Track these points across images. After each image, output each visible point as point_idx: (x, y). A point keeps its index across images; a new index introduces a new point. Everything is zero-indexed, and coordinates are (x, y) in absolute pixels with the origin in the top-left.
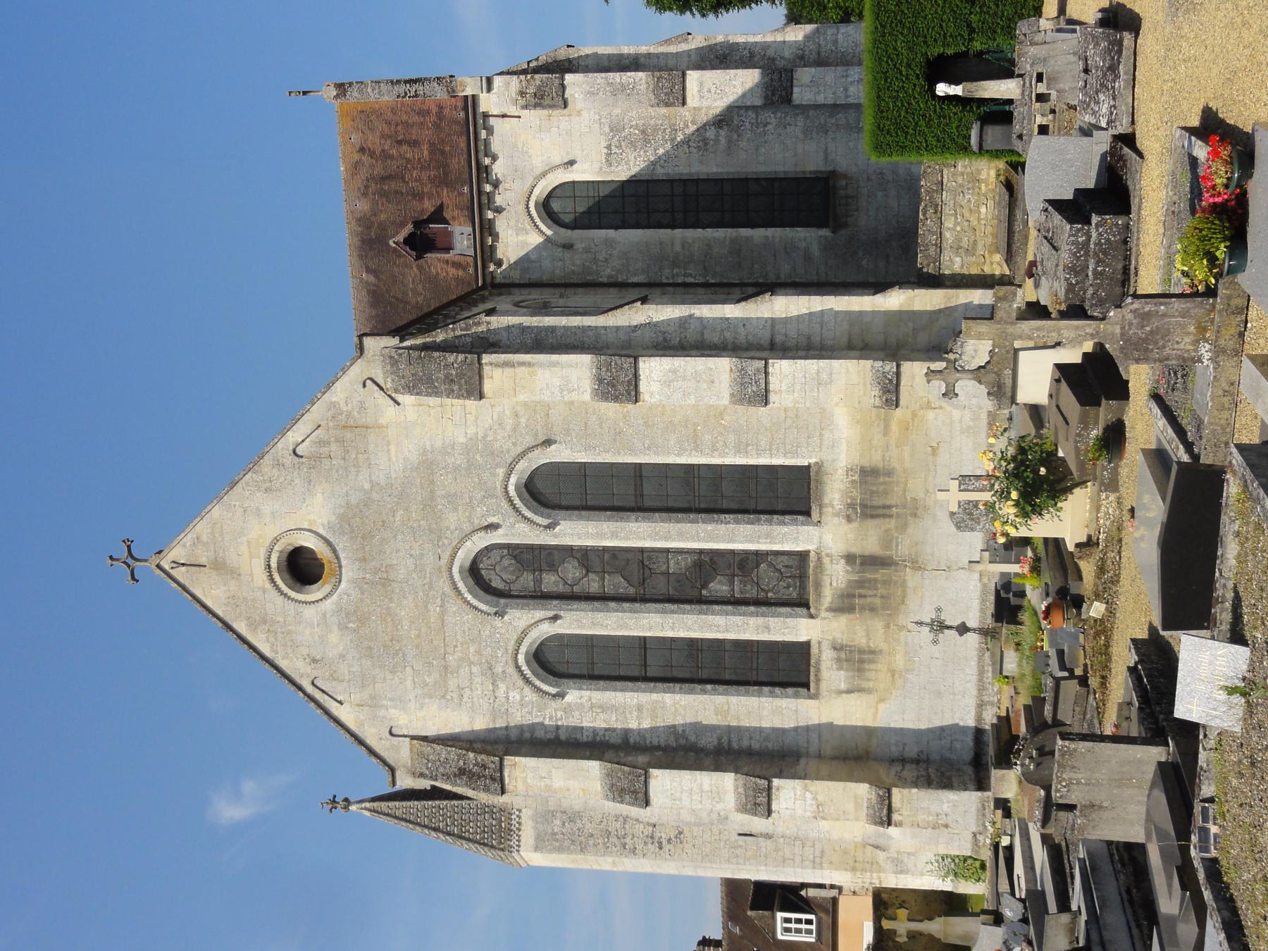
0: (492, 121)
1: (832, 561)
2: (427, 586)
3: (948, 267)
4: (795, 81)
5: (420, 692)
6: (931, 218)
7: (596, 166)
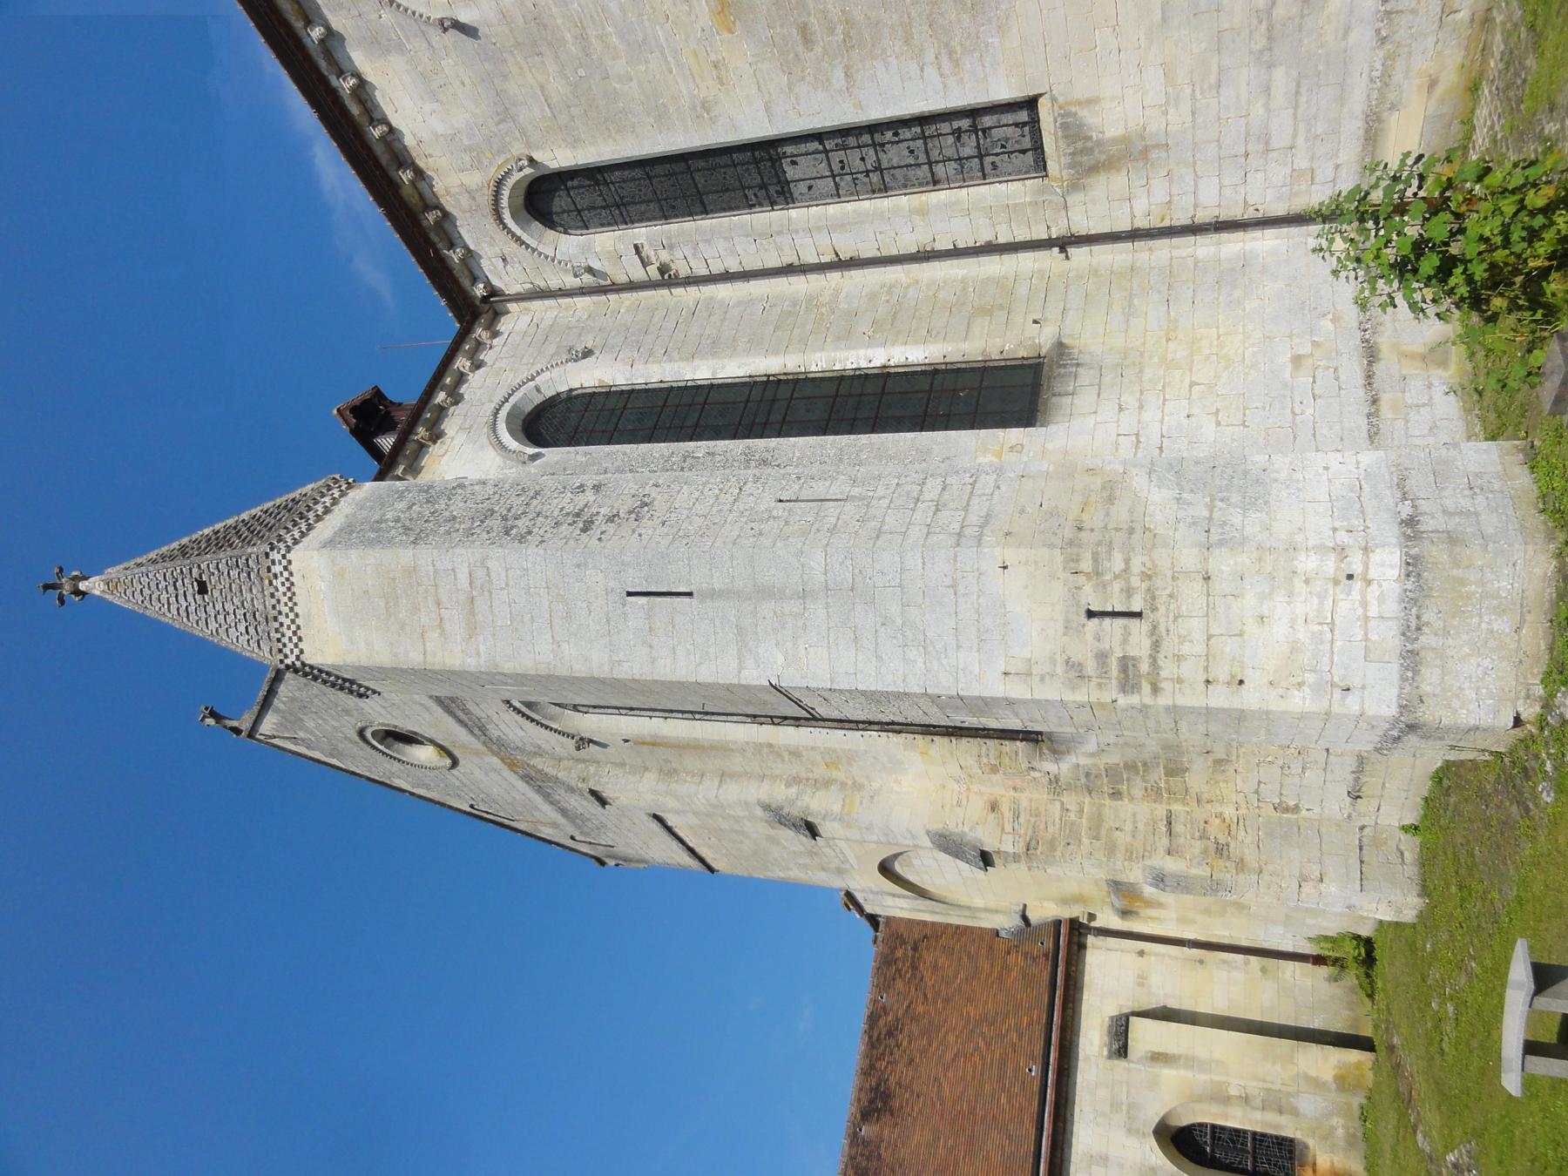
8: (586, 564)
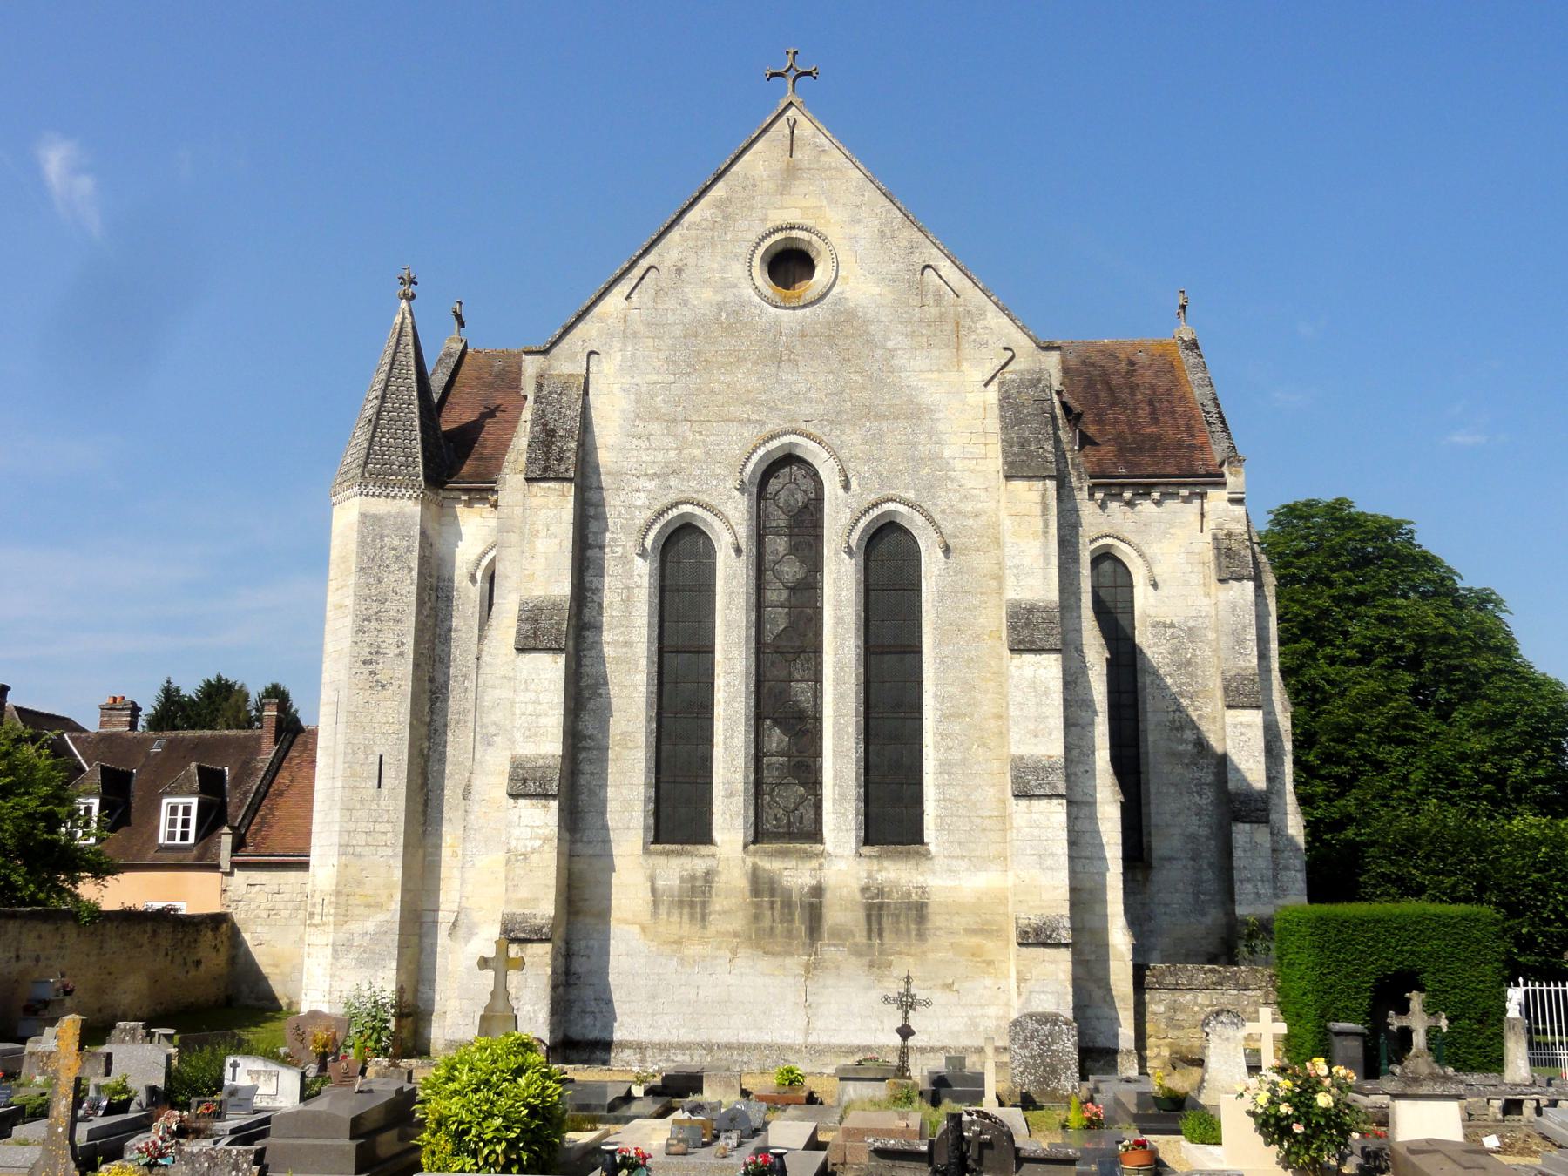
0: (1197, 502)
1: (815, 870)
2: (772, 404)
3: (1152, 998)
4: (1256, 826)
6: (1207, 978)
7: (1152, 612)
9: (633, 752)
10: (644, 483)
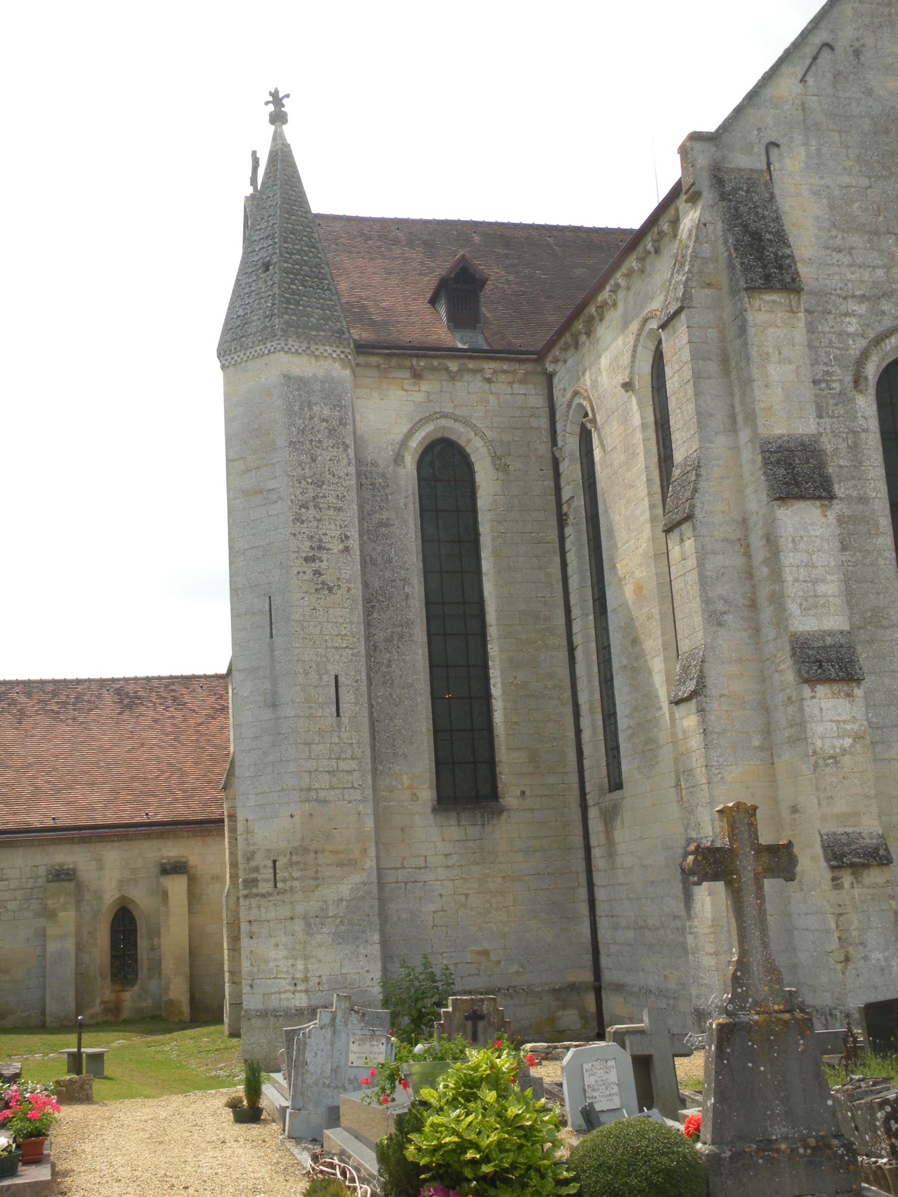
5: (836, 193)
8: (283, 568)
9: (888, 632)
10: (853, 306)
